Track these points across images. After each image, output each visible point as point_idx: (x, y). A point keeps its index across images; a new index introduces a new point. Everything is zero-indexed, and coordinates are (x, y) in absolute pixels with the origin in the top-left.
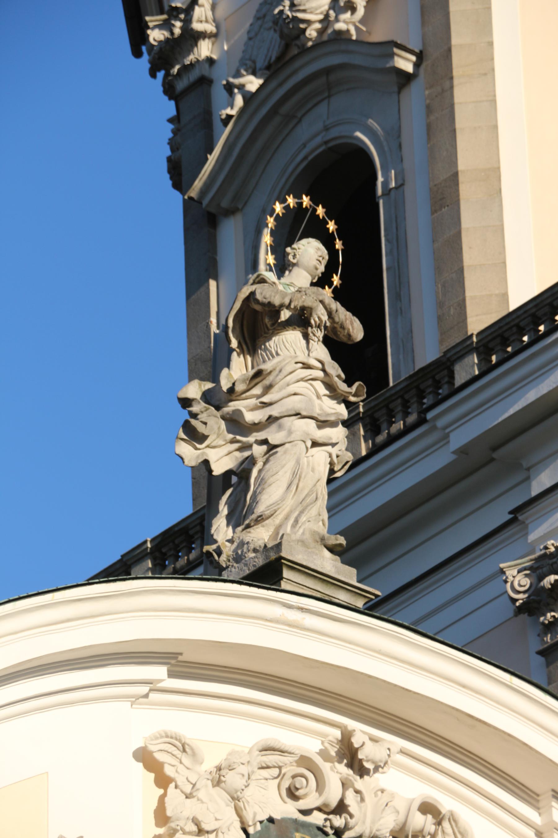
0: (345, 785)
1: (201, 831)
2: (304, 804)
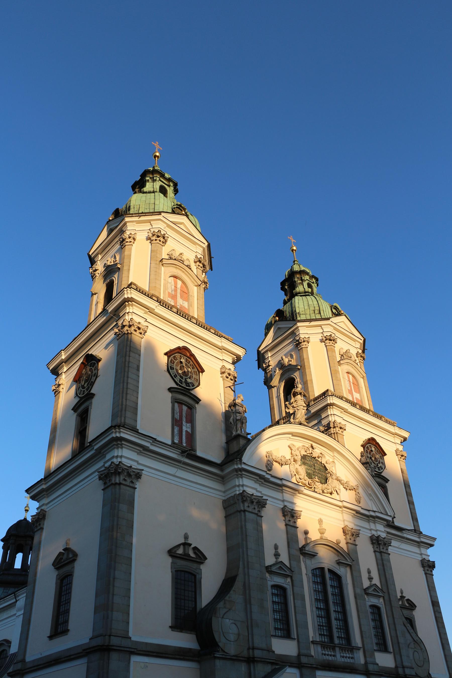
0: (312, 450)
1: (296, 456)
2: (307, 453)
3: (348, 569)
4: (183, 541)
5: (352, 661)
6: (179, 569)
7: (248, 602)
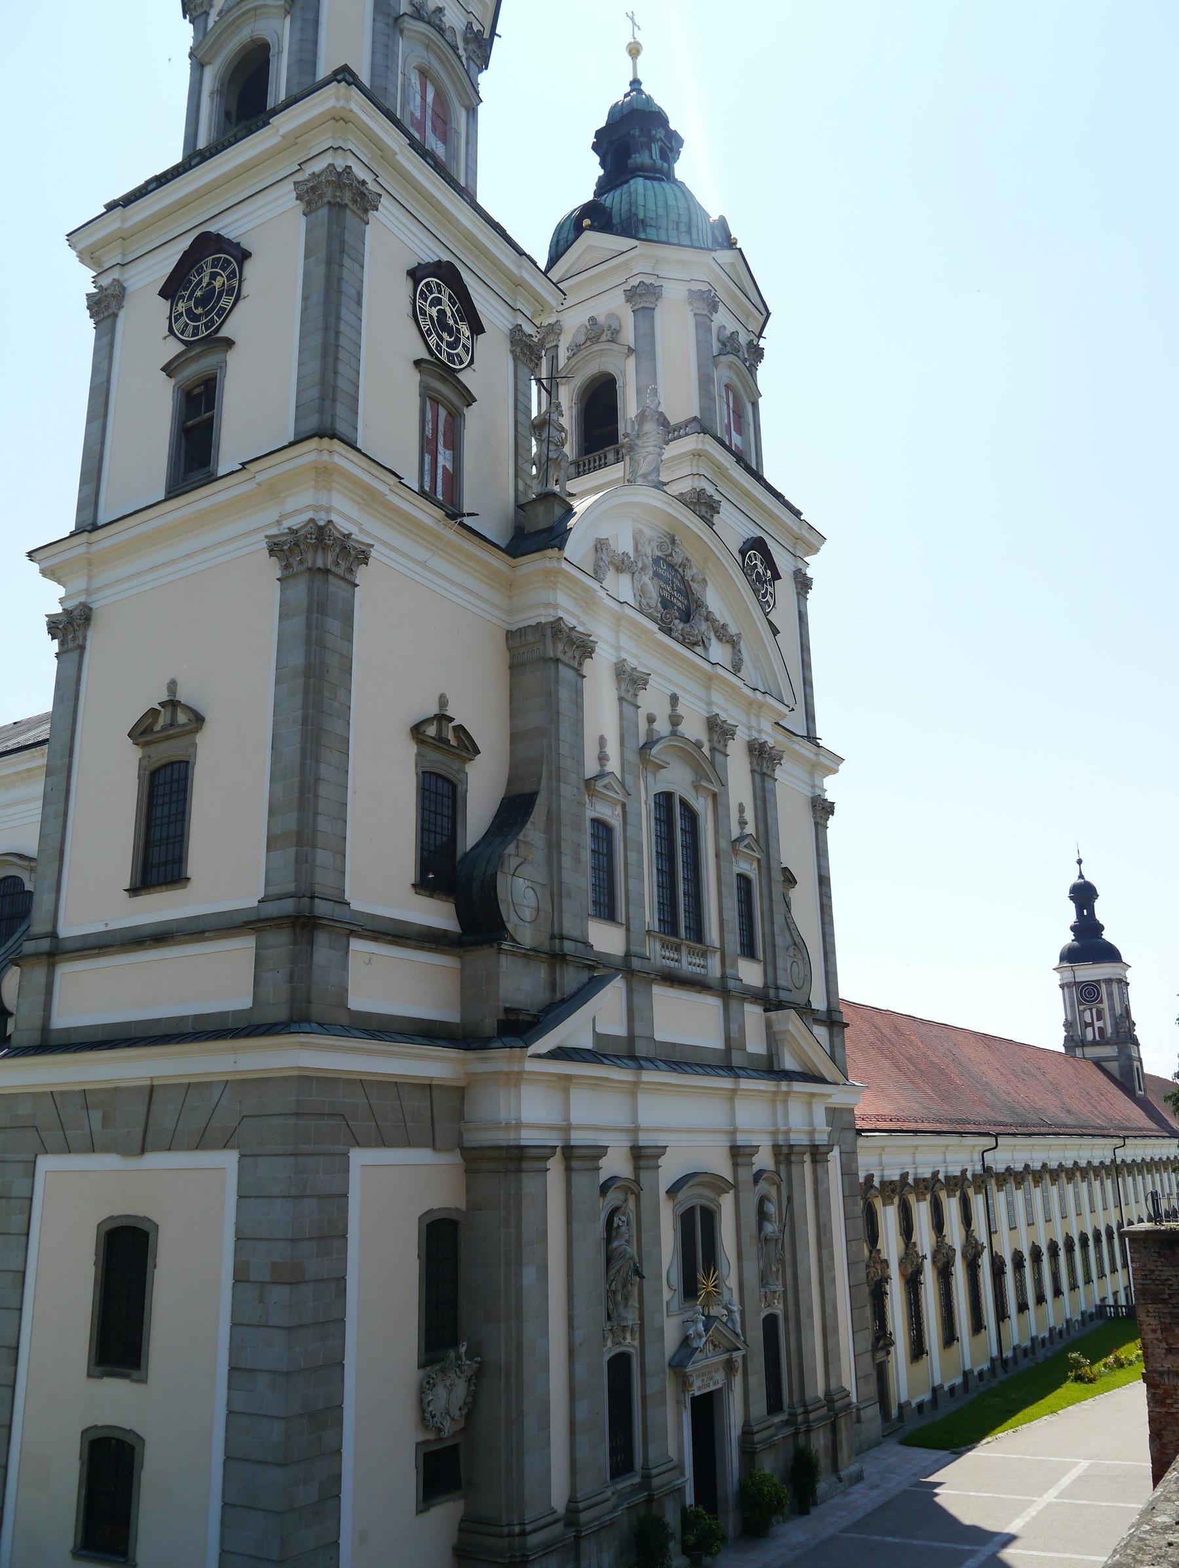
3: (710, 801)
4: (433, 710)
5: (703, 971)
6: (429, 769)
7: (554, 848)
